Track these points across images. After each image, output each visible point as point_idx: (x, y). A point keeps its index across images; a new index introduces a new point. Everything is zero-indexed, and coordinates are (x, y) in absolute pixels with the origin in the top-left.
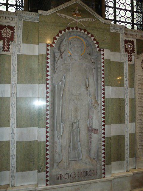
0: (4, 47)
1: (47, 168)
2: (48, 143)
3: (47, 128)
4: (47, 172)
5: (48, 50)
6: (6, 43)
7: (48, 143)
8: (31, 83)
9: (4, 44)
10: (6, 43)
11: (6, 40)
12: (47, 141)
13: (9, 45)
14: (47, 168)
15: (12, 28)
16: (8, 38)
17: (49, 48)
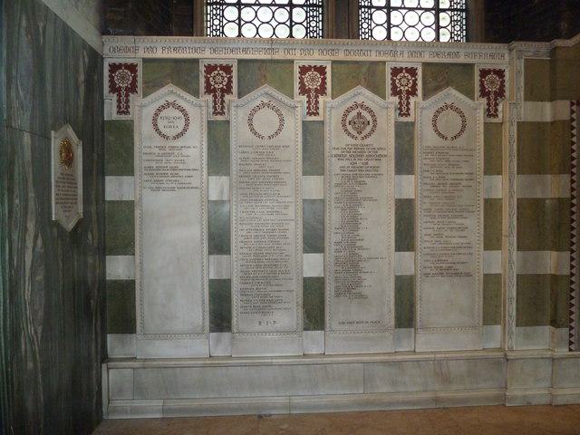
0: (488, 110)
1: (571, 321)
2: (573, 279)
3: (572, 251)
4: (571, 328)
5: (572, 112)
6: (493, 102)
7: (573, 279)
8: (540, 173)
9: (489, 104)
10: (493, 102)
11: (492, 97)
12: (572, 275)
13: (496, 104)
14: (571, 321)
15: (500, 73)
16: (495, 93)
17: (574, 108)
